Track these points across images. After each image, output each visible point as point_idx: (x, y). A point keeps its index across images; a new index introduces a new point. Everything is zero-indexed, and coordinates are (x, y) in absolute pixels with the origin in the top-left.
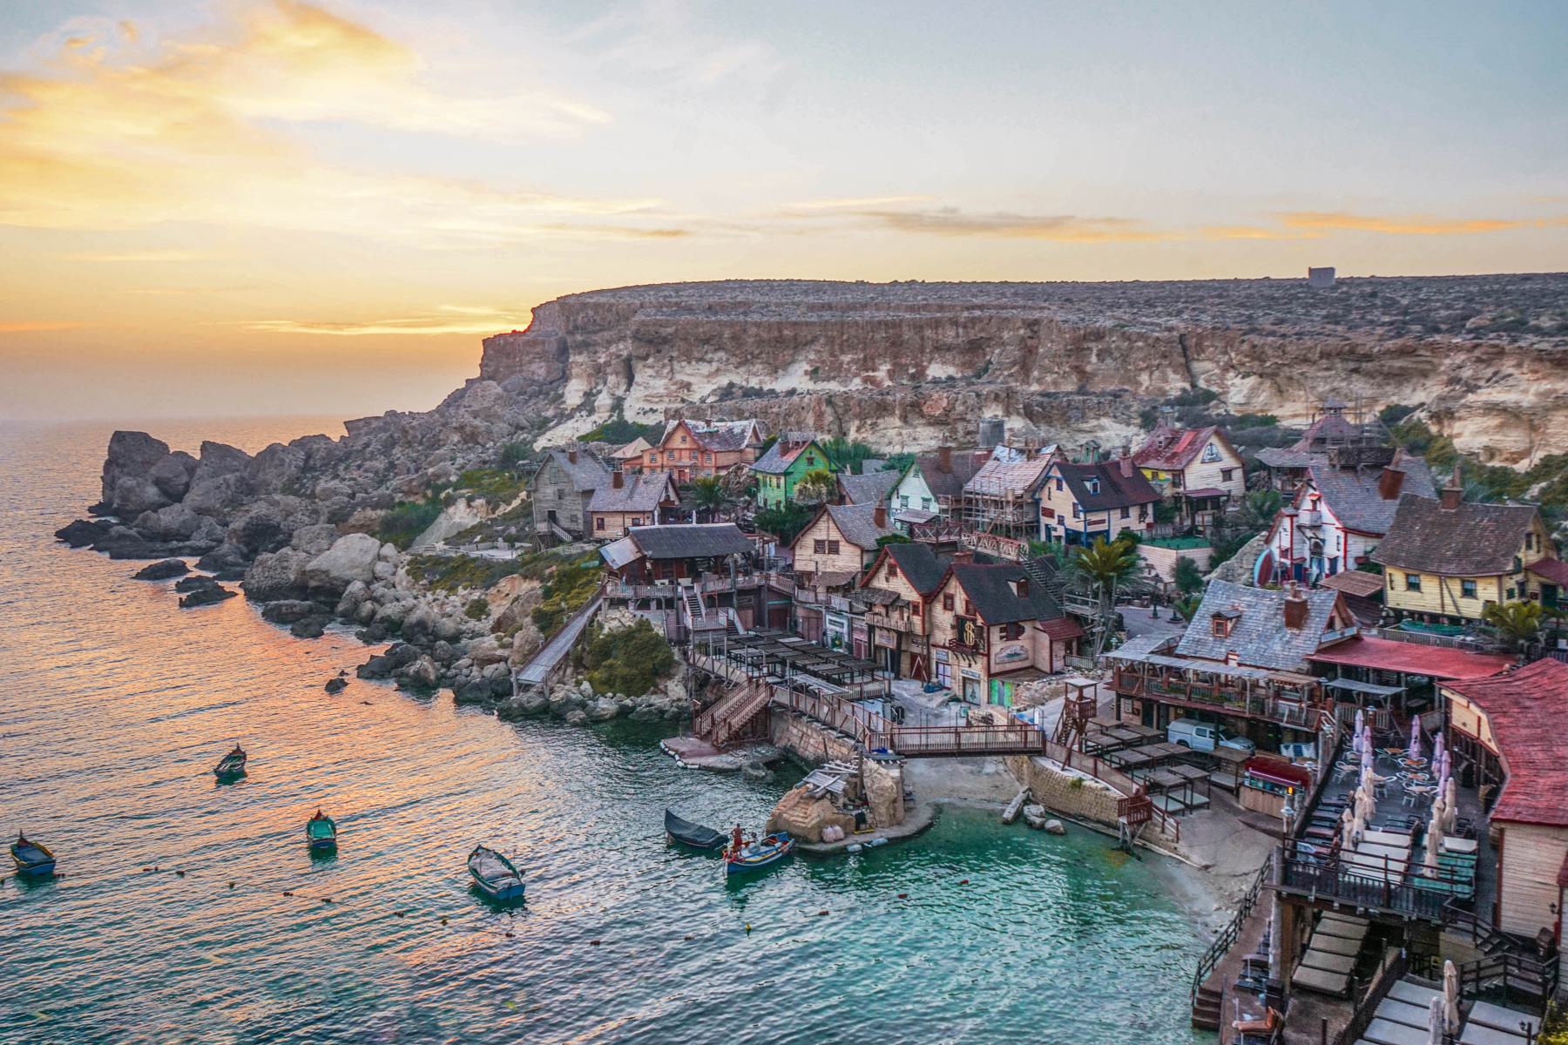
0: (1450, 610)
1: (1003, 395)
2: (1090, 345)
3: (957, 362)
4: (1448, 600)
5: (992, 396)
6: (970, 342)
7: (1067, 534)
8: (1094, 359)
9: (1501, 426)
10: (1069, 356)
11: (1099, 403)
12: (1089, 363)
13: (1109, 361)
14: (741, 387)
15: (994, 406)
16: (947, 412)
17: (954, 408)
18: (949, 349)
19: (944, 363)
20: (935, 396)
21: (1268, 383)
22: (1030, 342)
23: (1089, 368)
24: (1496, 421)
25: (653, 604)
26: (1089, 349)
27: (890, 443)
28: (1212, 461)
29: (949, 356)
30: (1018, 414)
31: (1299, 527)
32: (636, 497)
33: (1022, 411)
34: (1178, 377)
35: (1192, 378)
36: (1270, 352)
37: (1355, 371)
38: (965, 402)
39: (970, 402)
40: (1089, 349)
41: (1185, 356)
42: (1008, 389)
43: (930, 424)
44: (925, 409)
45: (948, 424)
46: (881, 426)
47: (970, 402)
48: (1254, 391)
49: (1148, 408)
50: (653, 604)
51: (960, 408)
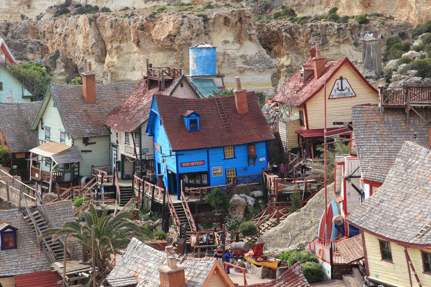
1: (234, 20)
5: (222, 20)
7: (168, 174)
11: (339, 29)
14: (79, 5)
15: (224, 31)
16: (171, 38)
17: (179, 32)
20: (165, 18)
27: (134, 69)
28: (345, 97)
30: (251, 40)
33: (254, 37)
38: (190, 27)
39: (196, 26)
42: (240, 13)
44: (153, 33)
45: (176, 51)
46: (125, 50)
47: (196, 26)
49: (396, 35)
51: (185, 33)
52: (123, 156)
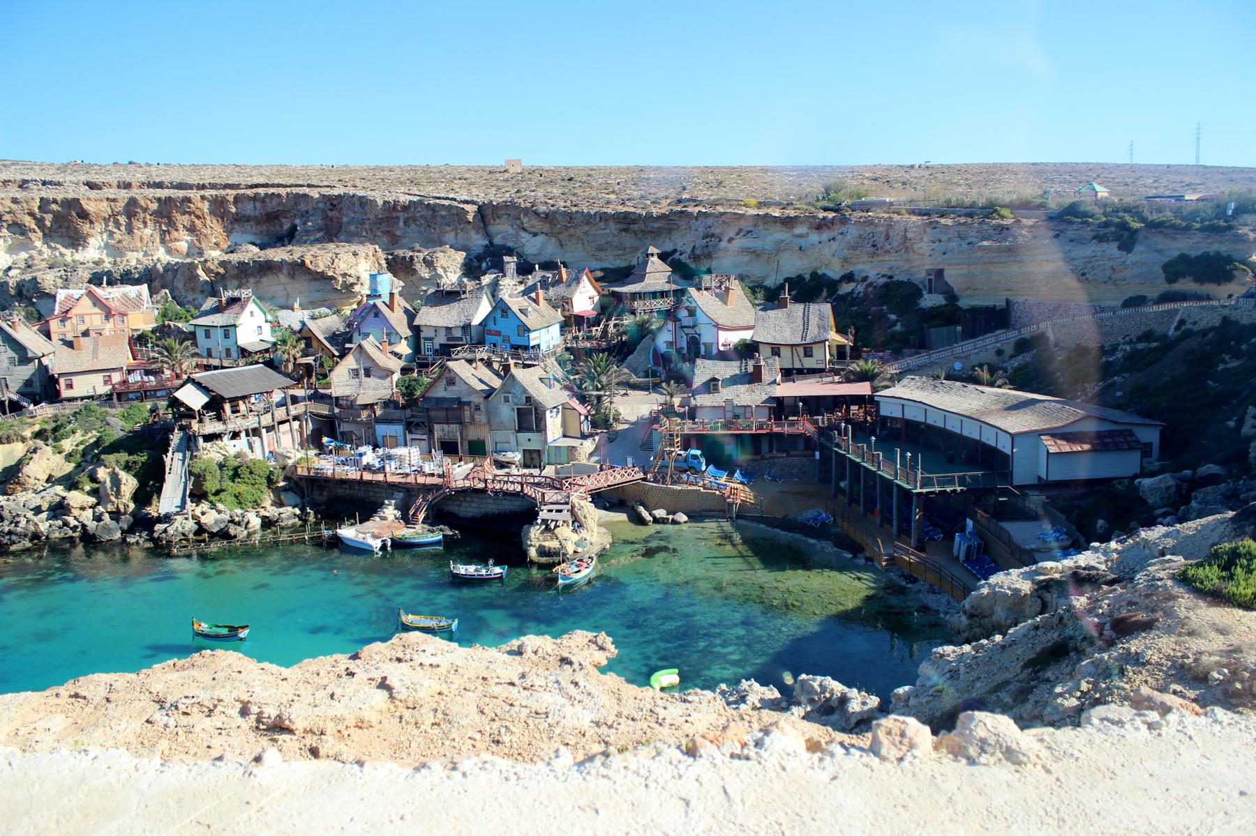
0: (798, 365)
2: (399, 214)
3: (254, 230)
4: (796, 359)
6: (268, 215)
8: (401, 224)
9: (750, 261)
10: (380, 223)
12: (399, 228)
13: (413, 226)
18: (247, 219)
19: (243, 232)
21: (553, 240)
22: (330, 214)
23: (398, 233)
24: (746, 259)
25: (243, 434)
26: (398, 218)
29: (247, 226)
31: (682, 327)
32: (101, 356)
34: (480, 236)
35: (488, 235)
36: (560, 218)
37: (626, 230)
40: (398, 218)
41: (484, 222)
43: (316, 279)
48: (544, 245)
50: (243, 434)
52: (441, 345)
